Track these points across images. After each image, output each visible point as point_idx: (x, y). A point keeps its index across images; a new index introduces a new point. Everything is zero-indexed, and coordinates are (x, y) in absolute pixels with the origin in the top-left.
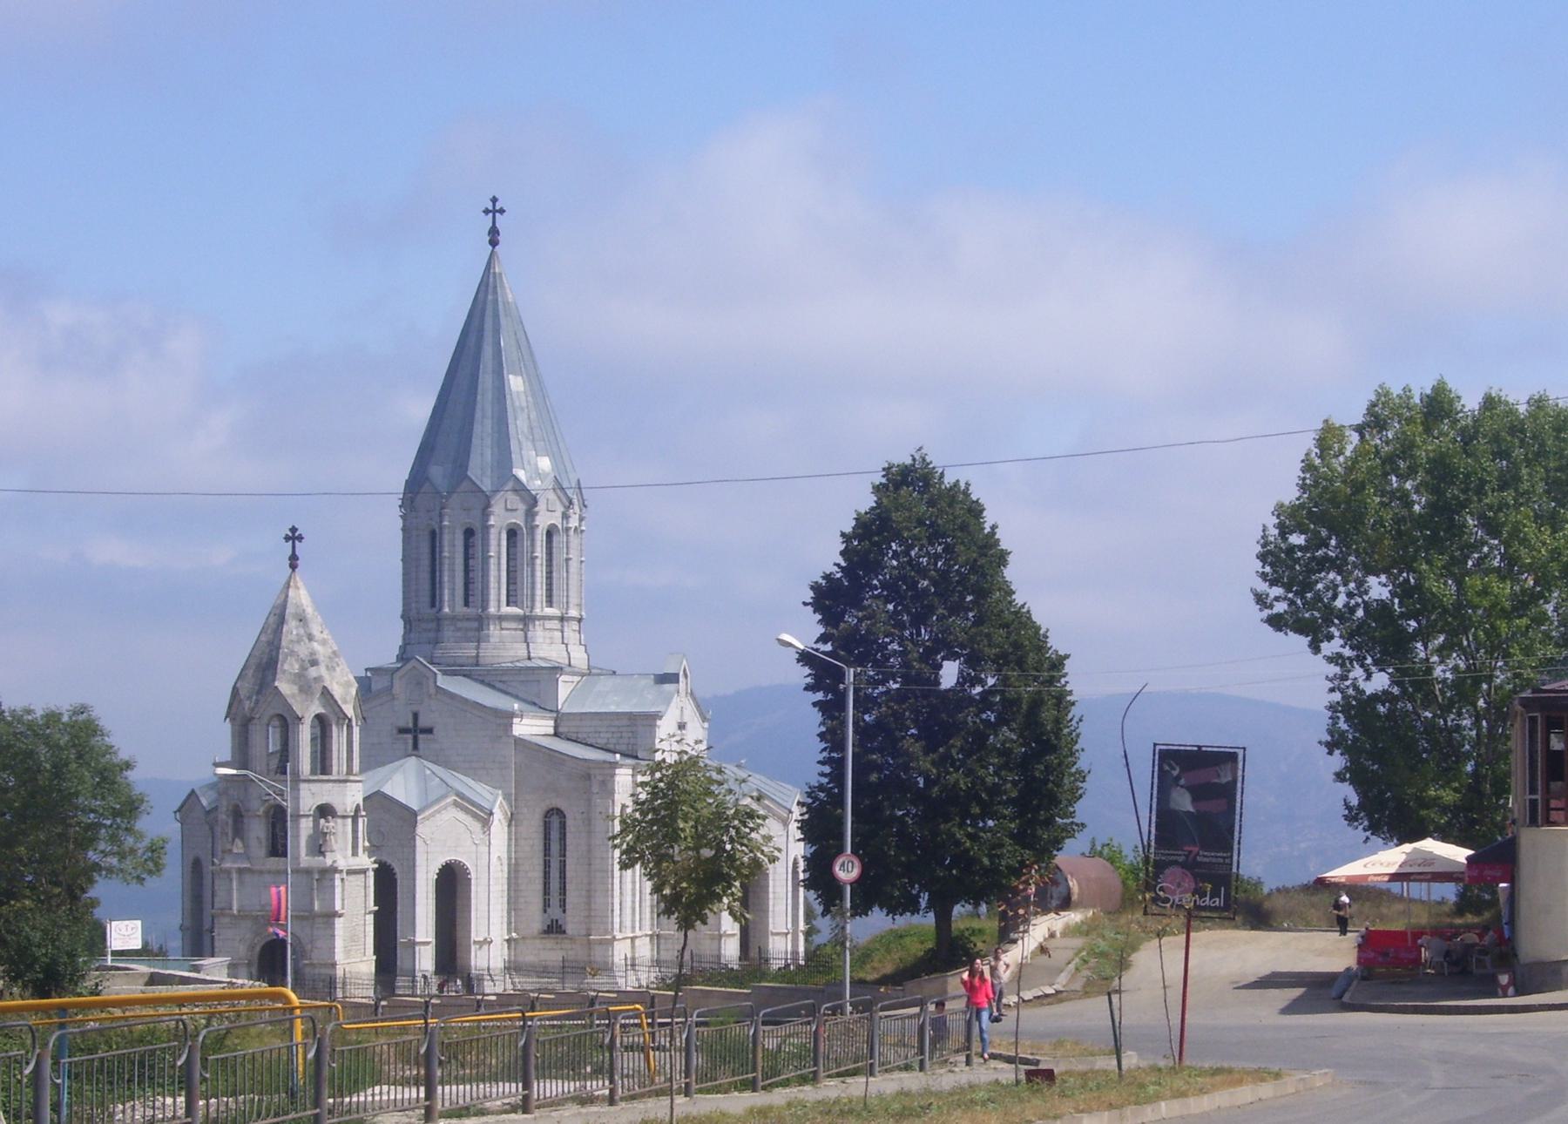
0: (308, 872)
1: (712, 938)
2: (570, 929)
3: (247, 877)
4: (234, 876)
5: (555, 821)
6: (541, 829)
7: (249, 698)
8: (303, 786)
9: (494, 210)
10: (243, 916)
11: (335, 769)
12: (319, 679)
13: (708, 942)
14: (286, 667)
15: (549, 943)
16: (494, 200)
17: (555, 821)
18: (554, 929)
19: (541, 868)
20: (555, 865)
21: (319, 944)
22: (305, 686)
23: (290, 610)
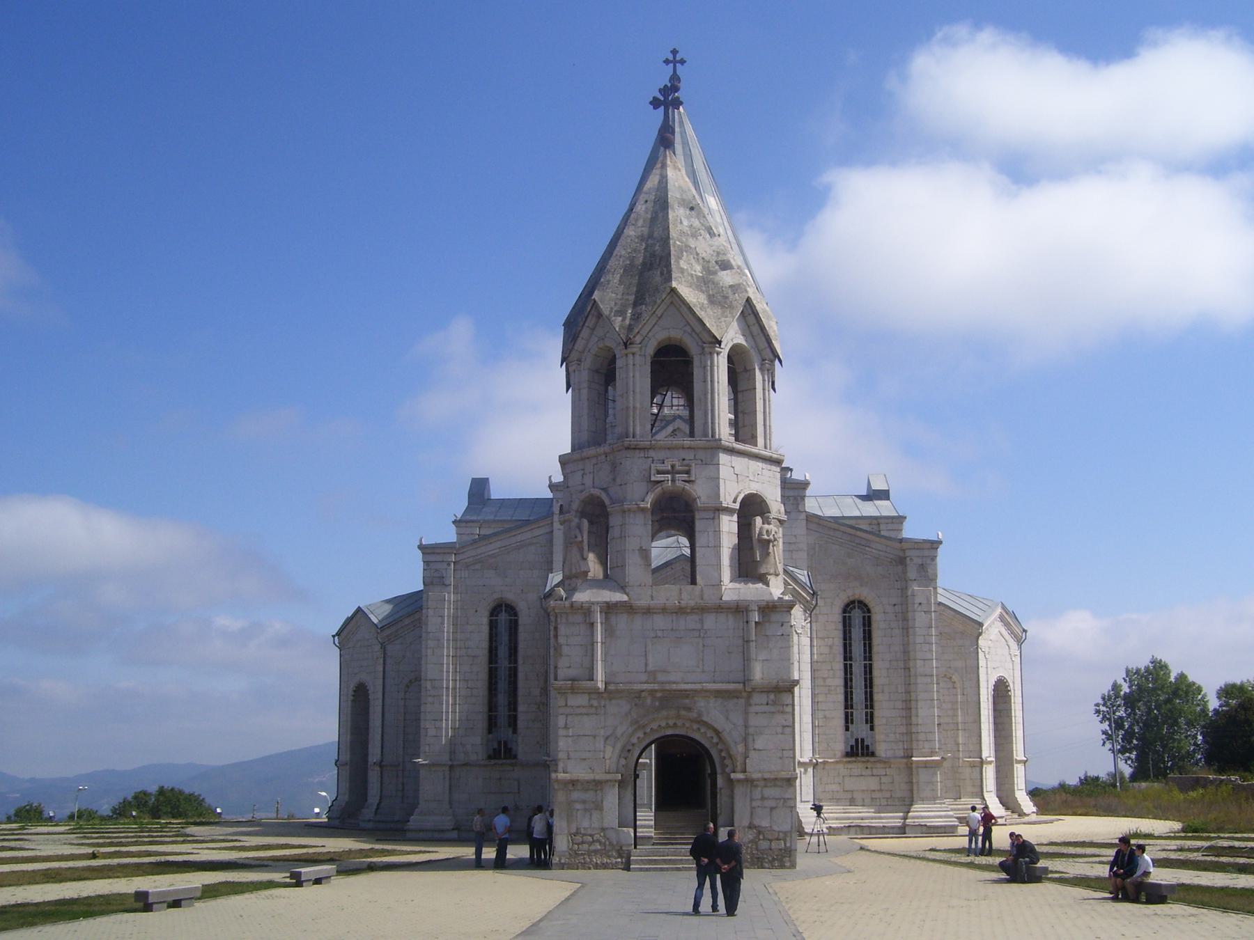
0: (739, 609)
1: (972, 765)
2: (882, 749)
3: (621, 621)
4: (598, 618)
5: (857, 615)
6: (840, 626)
7: (621, 313)
8: (724, 458)
9: (675, 60)
10: (610, 693)
11: (760, 440)
12: (735, 288)
13: (968, 770)
14: (683, 264)
15: (857, 767)
16: (674, 52)
17: (857, 615)
18: (859, 750)
19: (841, 674)
20: (858, 669)
21: (760, 743)
22: (719, 299)
23: (673, 195)
